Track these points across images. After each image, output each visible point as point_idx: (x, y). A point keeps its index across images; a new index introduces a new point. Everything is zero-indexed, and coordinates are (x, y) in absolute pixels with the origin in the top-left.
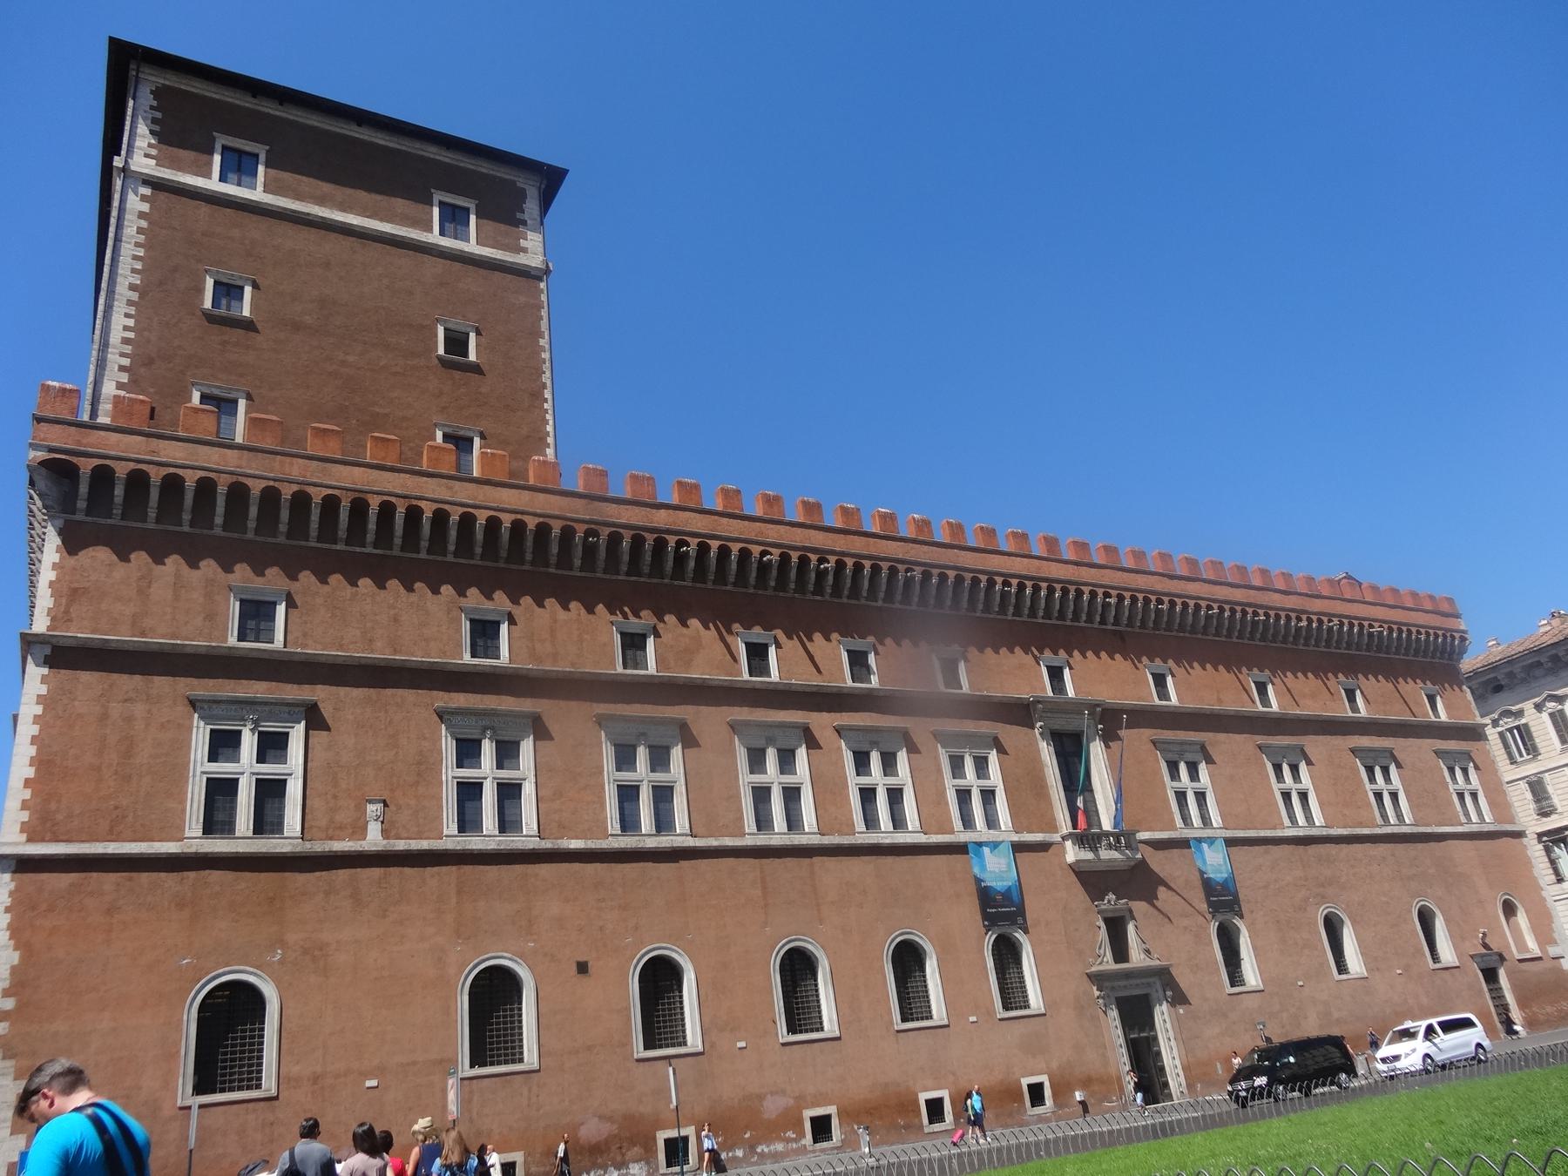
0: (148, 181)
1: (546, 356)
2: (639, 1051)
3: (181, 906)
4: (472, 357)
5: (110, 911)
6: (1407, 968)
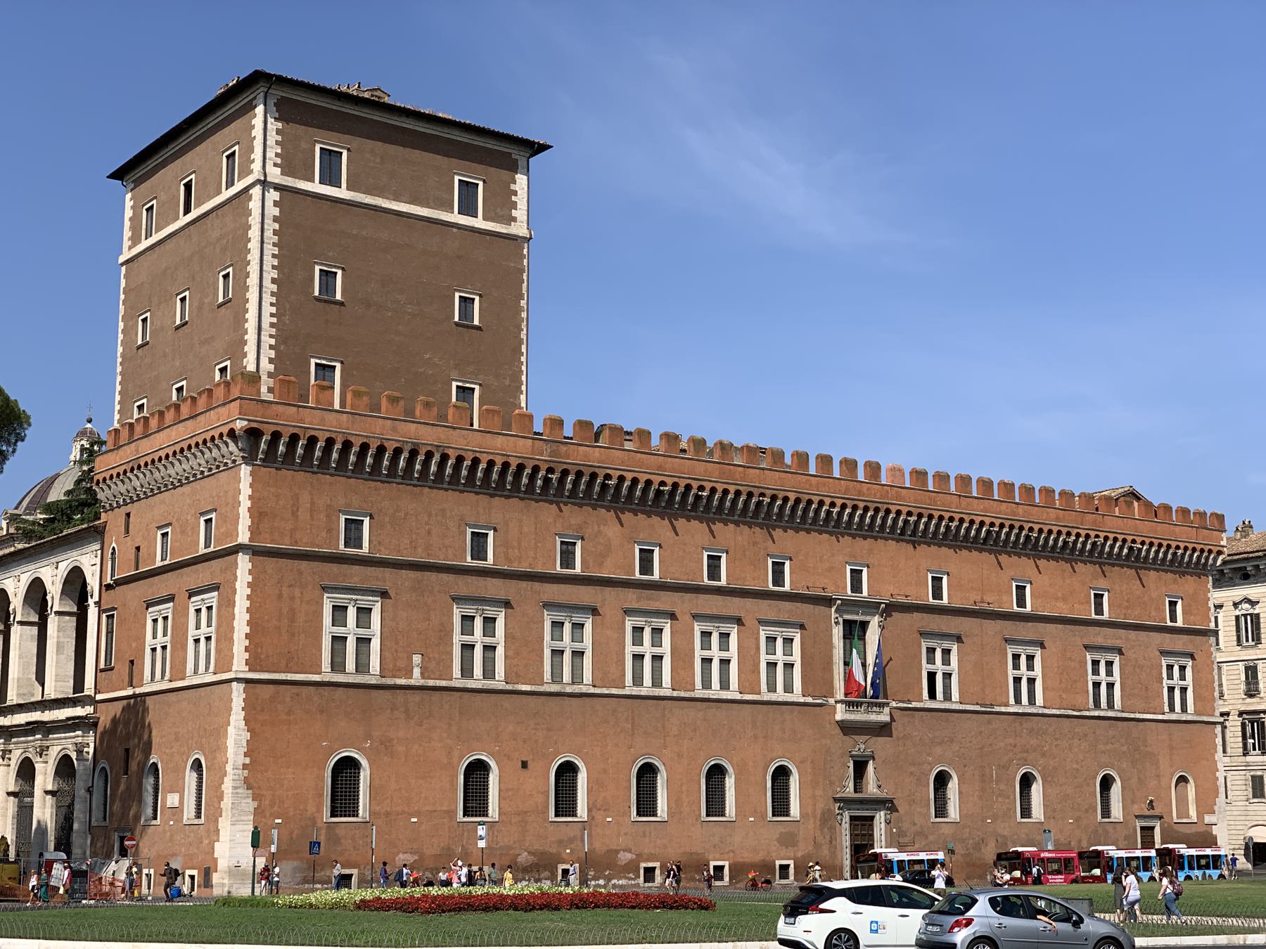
0: (277, 187)
3: (322, 712)
4: (476, 322)
5: (288, 713)
6: (1077, 820)
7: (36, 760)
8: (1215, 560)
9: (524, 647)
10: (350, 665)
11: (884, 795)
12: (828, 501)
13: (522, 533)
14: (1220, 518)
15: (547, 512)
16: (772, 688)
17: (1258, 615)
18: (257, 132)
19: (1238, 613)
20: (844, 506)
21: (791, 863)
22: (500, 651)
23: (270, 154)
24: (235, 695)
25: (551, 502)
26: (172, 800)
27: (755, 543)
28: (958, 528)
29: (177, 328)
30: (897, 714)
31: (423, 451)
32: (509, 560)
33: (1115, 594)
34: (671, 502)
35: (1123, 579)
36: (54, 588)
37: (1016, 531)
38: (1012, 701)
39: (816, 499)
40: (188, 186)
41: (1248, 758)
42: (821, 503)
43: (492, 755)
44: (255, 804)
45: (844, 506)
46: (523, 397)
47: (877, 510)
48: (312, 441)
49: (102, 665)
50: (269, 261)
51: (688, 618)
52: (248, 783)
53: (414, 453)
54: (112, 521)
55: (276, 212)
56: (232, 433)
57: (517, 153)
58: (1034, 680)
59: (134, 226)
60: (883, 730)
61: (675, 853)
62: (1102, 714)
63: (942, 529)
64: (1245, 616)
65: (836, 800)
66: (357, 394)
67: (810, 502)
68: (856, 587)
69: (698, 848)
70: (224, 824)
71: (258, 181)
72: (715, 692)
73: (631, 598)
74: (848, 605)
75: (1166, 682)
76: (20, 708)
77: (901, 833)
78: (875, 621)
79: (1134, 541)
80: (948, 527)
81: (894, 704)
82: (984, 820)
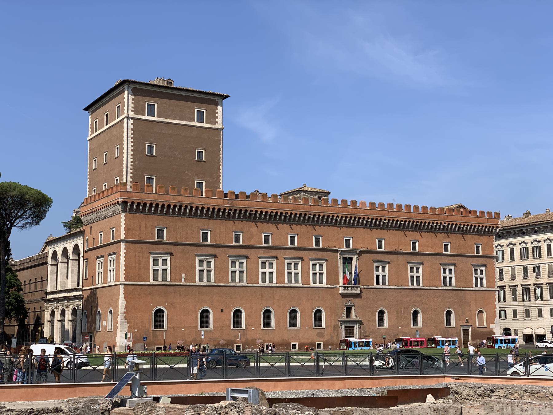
0: (132, 119)
1: (221, 156)
2: (232, 328)
3: (150, 294)
4: (204, 160)
5: (139, 295)
6: (436, 327)
7: (66, 309)
8: (496, 230)
9: (221, 270)
10: (160, 278)
11: (358, 319)
12: (336, 215)
13: (220, 232)
14: (498, 214)
15: (230, 224)
16: (315, 282)
17: (540, 246)
18: (126, 100)
19: (521, 247)
20: (342, 217)
21: (322, 343)
22: (213, 272)
23: (130, 107)
24: (121, 289)
25: (231, 220)
26: (104, 323)
27: (308, 232)
28: (388, 223)
29: (104, 164)
30: (363, 290)
31: (184, 206)
32: (216, 241)
33: (453, 244)
34: (276, 218)
35: (457, 239)
36: (70, 251)
37: (411, 223)
38: (410, 284)
39: (331, 215)
40: (107, 115)
41: (525, 302)
42: (333, 216)
43: (210, 307)
44: (128, 325)
45: (342, 217)
46: (221, 184)
47: (355, 218)
48: (145, 204)
49: (84, 278)
50: (130, 144)
51: (282, 258)
52: (126, 318)
53: (181, 207)
54: (87, 228)
55: (132, 127)
56: (118, 202)
57: (217, 99)
58: (419, 276)
59: (91, 127)
60: (358, 296)
61: (277, 340)
62: (447, 288)
63: (382, 223)
64: (536, 247)
65: (339, 321)
66: (160, 187)
67: (329, 216)
68: (348, 245)
69: (286, 338)
70: (118, 331)
71: (126, 117)
72: (293, 284)
73: (261, 252)
74: (344, 252)
75: (474, 276)
76: (61, 292)
77: (365, 332)
78: (355, 258)
79: (460, 224)
80: (384, 223)
81: (362, 287)
82: (398, 327)
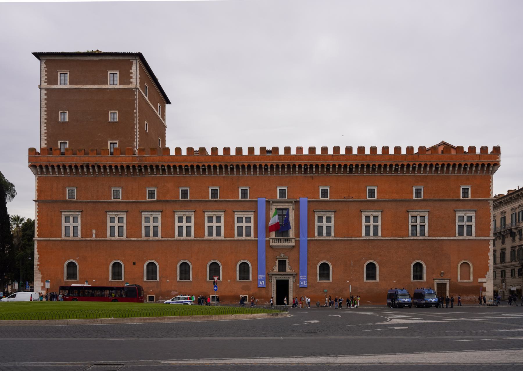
0: (46, 89)
21: (247, 296)
43: (122, 261)
52: (39, 269)
55: (46, 97)
